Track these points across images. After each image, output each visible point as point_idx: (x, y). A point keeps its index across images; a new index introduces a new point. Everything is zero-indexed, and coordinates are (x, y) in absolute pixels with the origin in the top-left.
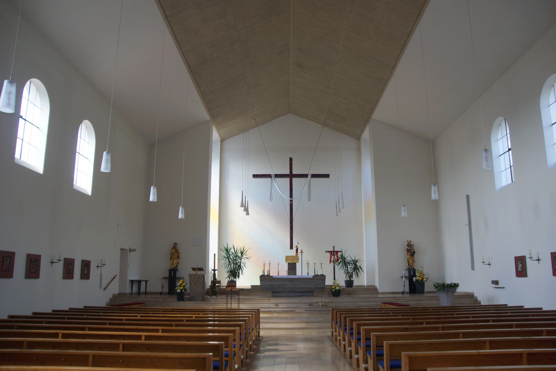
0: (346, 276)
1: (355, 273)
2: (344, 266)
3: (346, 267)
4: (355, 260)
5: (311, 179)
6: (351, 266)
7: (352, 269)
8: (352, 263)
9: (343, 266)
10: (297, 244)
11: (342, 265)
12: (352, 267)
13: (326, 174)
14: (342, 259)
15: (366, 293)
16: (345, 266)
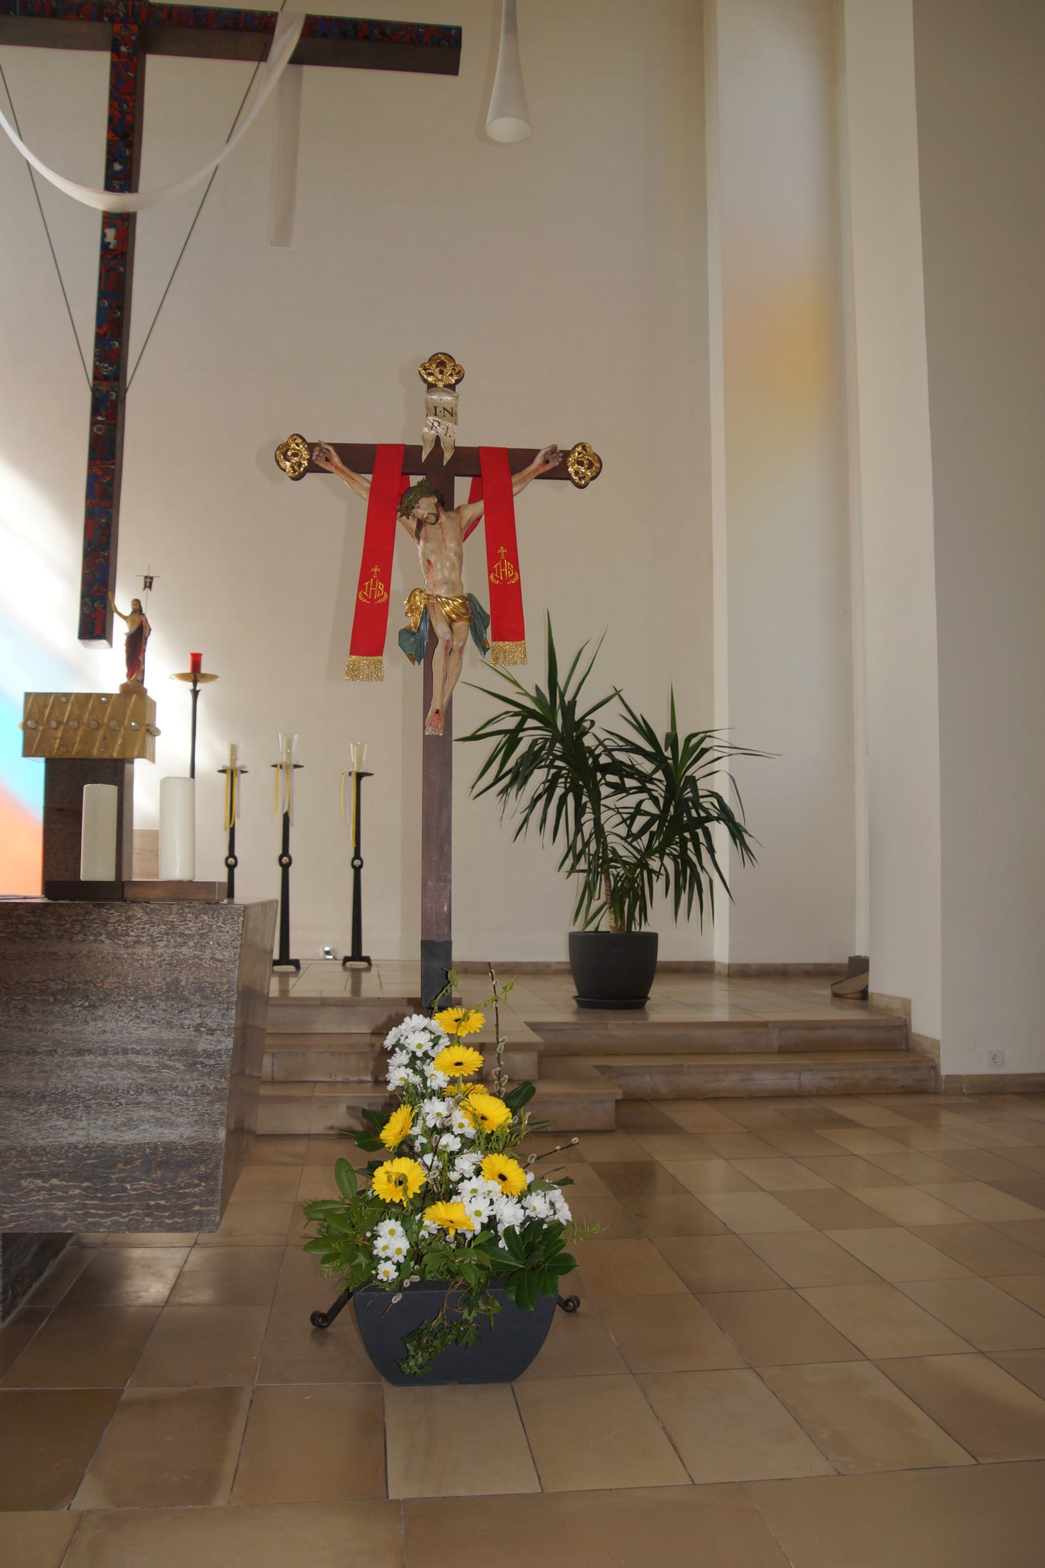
0: (589, 888)
1: (668, 862)
2: (563, 800)
3: (580, 811)
4: (672, 739)
5: (311, 73)
6: (632, 800)
7: (640, 821)
8: (646, 766)
9: (559, 791)
10: (141, 595)
11: (550, 791)
12: (638, 810)
13: (428, 27)
14: (548, 723)
15: (809, 1080)
16: (570, 799)
